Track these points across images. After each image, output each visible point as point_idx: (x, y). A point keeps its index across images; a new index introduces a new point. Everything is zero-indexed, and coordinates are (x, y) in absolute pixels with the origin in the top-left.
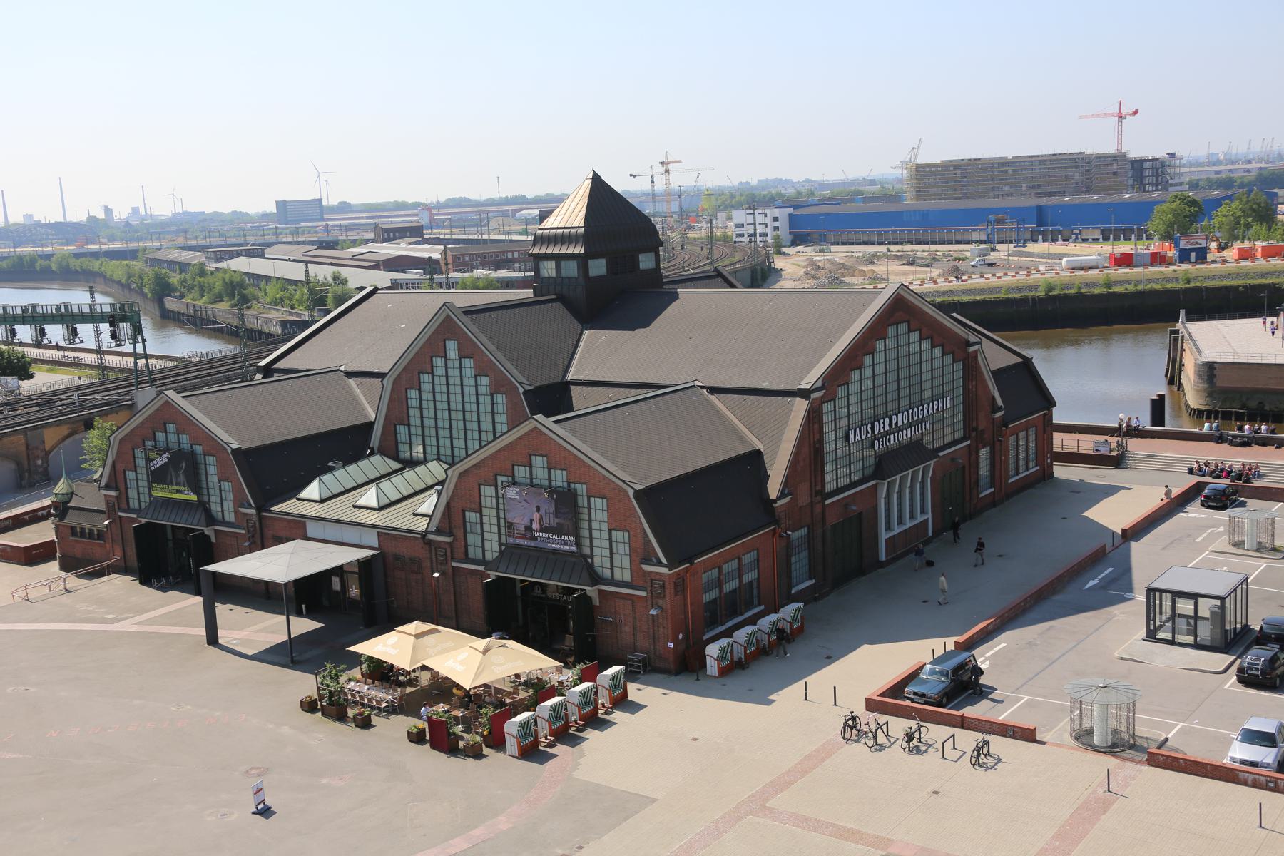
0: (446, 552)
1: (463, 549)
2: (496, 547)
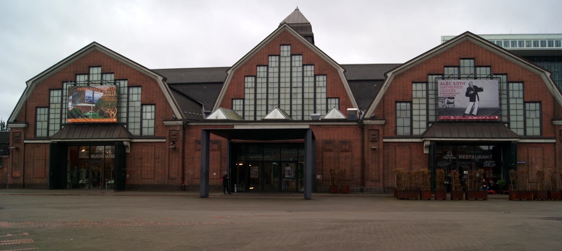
0: (378, 133)
1: (393, 129)
2: (424, 124)
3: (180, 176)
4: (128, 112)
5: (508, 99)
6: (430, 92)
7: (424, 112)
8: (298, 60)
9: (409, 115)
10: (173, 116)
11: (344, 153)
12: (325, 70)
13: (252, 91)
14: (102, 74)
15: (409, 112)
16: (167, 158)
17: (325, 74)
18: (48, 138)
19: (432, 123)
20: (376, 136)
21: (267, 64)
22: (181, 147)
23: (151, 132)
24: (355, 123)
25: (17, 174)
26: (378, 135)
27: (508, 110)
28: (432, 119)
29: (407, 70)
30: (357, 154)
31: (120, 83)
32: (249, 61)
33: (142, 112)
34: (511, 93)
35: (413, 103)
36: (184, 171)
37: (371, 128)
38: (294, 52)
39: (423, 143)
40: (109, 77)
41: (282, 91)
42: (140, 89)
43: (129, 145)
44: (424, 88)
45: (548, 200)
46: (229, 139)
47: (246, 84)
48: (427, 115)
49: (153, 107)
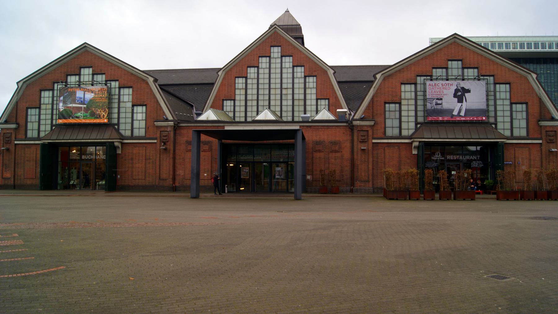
1: (383, 130)
2: (412, 125)
3: (171, 177)
4: (119, 113)
5: (495, 100)
6: (419, 93)
7: (413, 113)
8: (288, 62)
9: (398, 116)
10: (164, 116)
11: (334, 154)
12: (315, 71)
13: (243, 92)
14: (93, 75)
15: (397, 113)
16: (158, 159)
17: (315, 75)
18: (39, 138)
19: (421, 124)
20: (366, 137)
21: (257, 66)
22: (172, 148)
23: (142, 133)
24: (345, 124)
25: (8, 175)
26: (368, 136)
27: (496, 111)
28: (420, 120)
29: (396, 72)
30: (346, 153)
31: (111, 84)
32: (239, 62)
33: (133, 113)
34: (498, 94)
35: (402, 104)
36: (175, 172)
37: (361, 129)
38: (285, 54)
39: (411, 143)
40: (100, 78)
41: (272, 92)
42: (131, 90)
43: (120, 146)
44: (413, 89)
45: (534, 200)
46: (220, 140)
47: (237, 85)
48: (416, 116)
49: (144, 108)
